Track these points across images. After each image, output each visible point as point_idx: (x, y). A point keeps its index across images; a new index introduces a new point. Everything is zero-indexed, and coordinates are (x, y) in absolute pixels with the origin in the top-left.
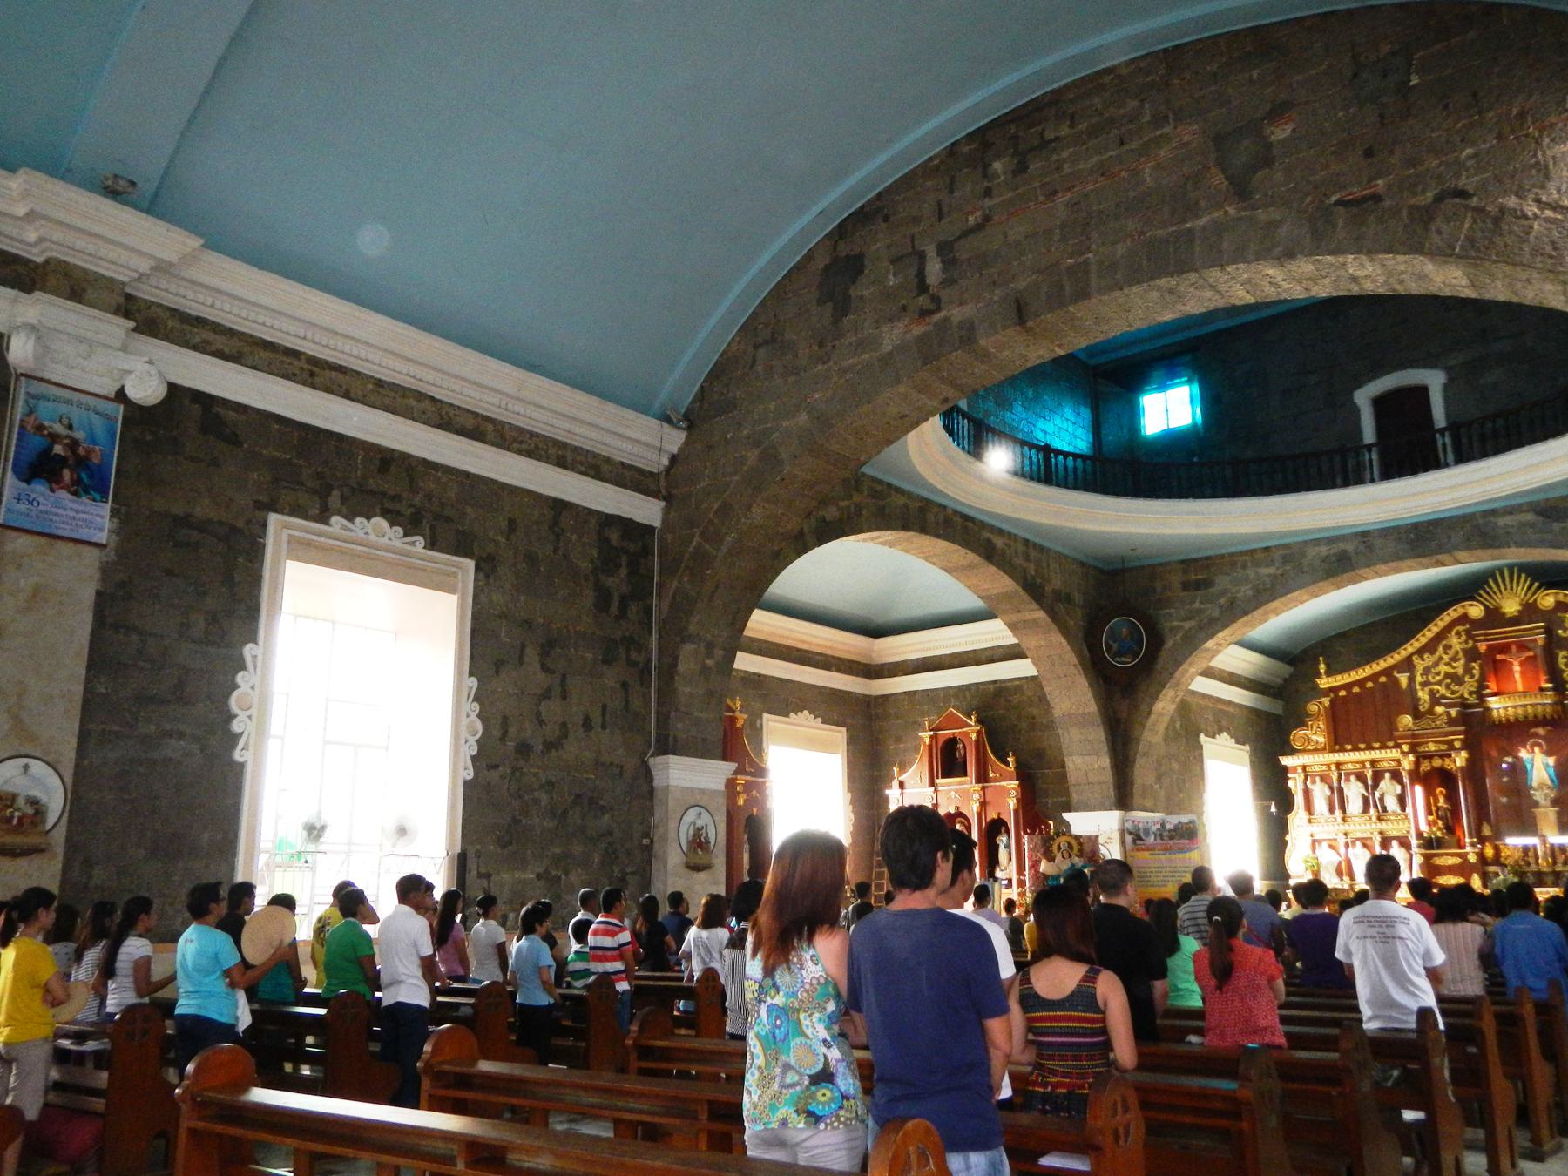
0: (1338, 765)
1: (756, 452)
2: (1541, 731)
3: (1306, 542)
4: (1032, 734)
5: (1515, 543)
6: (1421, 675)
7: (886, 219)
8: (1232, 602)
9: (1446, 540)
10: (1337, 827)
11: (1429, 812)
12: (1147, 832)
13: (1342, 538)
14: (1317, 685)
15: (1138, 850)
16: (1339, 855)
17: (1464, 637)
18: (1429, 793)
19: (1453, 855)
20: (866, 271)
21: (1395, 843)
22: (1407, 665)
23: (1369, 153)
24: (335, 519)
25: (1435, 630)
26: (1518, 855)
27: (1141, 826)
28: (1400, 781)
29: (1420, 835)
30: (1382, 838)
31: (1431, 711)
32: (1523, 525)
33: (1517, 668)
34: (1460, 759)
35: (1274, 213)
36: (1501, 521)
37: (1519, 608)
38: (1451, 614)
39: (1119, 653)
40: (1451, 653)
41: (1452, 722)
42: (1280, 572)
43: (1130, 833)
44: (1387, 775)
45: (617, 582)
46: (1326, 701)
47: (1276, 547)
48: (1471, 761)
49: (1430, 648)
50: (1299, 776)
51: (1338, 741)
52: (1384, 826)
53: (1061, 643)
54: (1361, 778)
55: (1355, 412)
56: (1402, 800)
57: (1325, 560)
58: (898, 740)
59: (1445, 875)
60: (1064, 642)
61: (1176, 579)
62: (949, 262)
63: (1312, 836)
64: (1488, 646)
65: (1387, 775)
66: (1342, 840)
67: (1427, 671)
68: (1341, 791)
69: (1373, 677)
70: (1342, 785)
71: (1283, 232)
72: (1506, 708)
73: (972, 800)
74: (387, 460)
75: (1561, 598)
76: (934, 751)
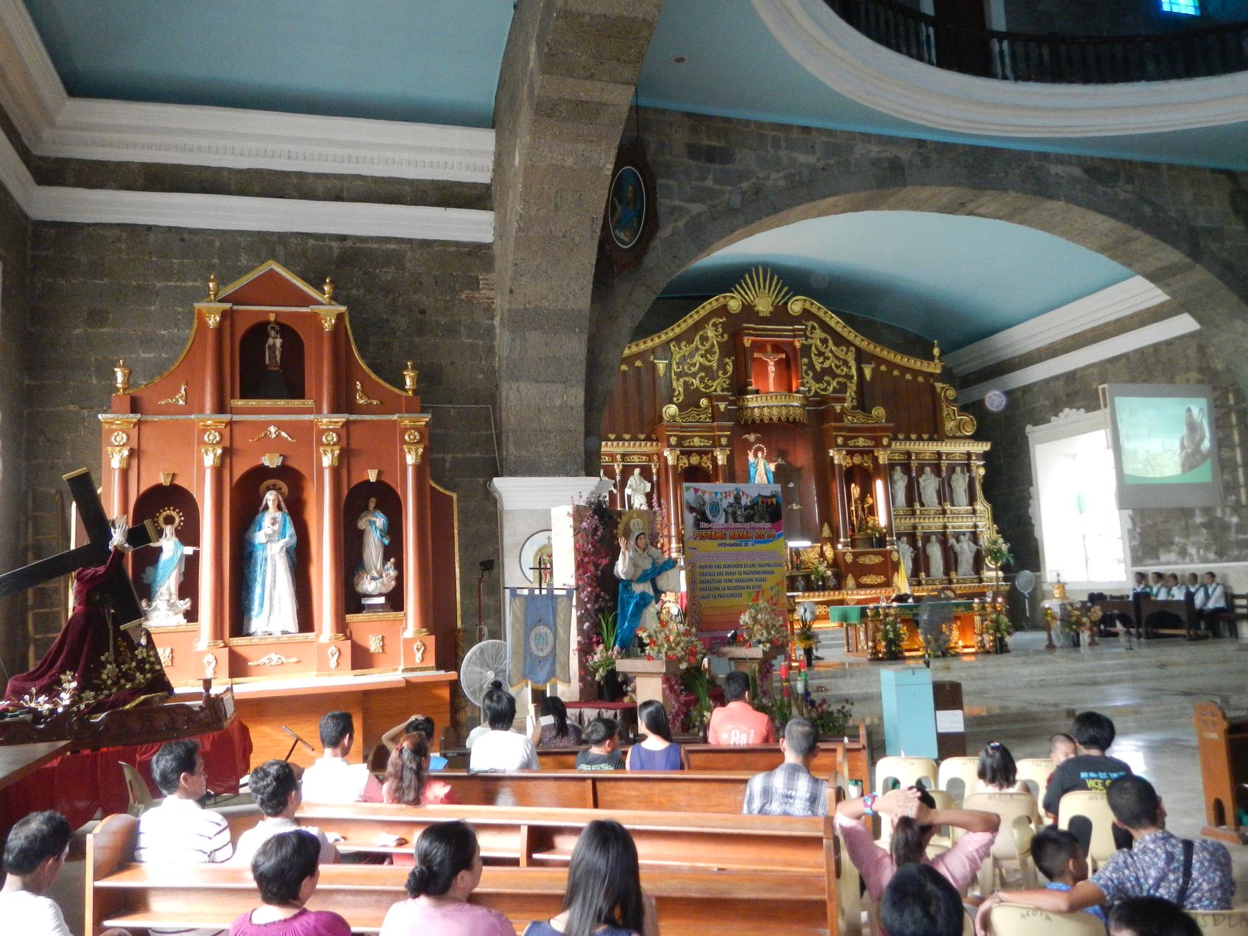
3: (852, 135)
4: (417, 340)
5: (1066, 197)
6: (678, 364)
9: (1003, 174)
12: (715, 507)
15: (702, 538)
17: (720, 330)
25: (696, 317)
27: (707, 497)
28: (650, 481)
33: (772, 368)
34: (721, 459)
37: (771, 309)
40: (708, 345)
42: (821, 164)
43: (692, 509)
44: (637, 471)
47: (818, 129)
49: (687, 336)
53: (600, 169)
57: (875, 163)
58: (96, 317)
61: (680, 138)
64: (753, 342)
65: (637, 471)
73: (322, 444)
75: (808, 306)
76: (227, 341)
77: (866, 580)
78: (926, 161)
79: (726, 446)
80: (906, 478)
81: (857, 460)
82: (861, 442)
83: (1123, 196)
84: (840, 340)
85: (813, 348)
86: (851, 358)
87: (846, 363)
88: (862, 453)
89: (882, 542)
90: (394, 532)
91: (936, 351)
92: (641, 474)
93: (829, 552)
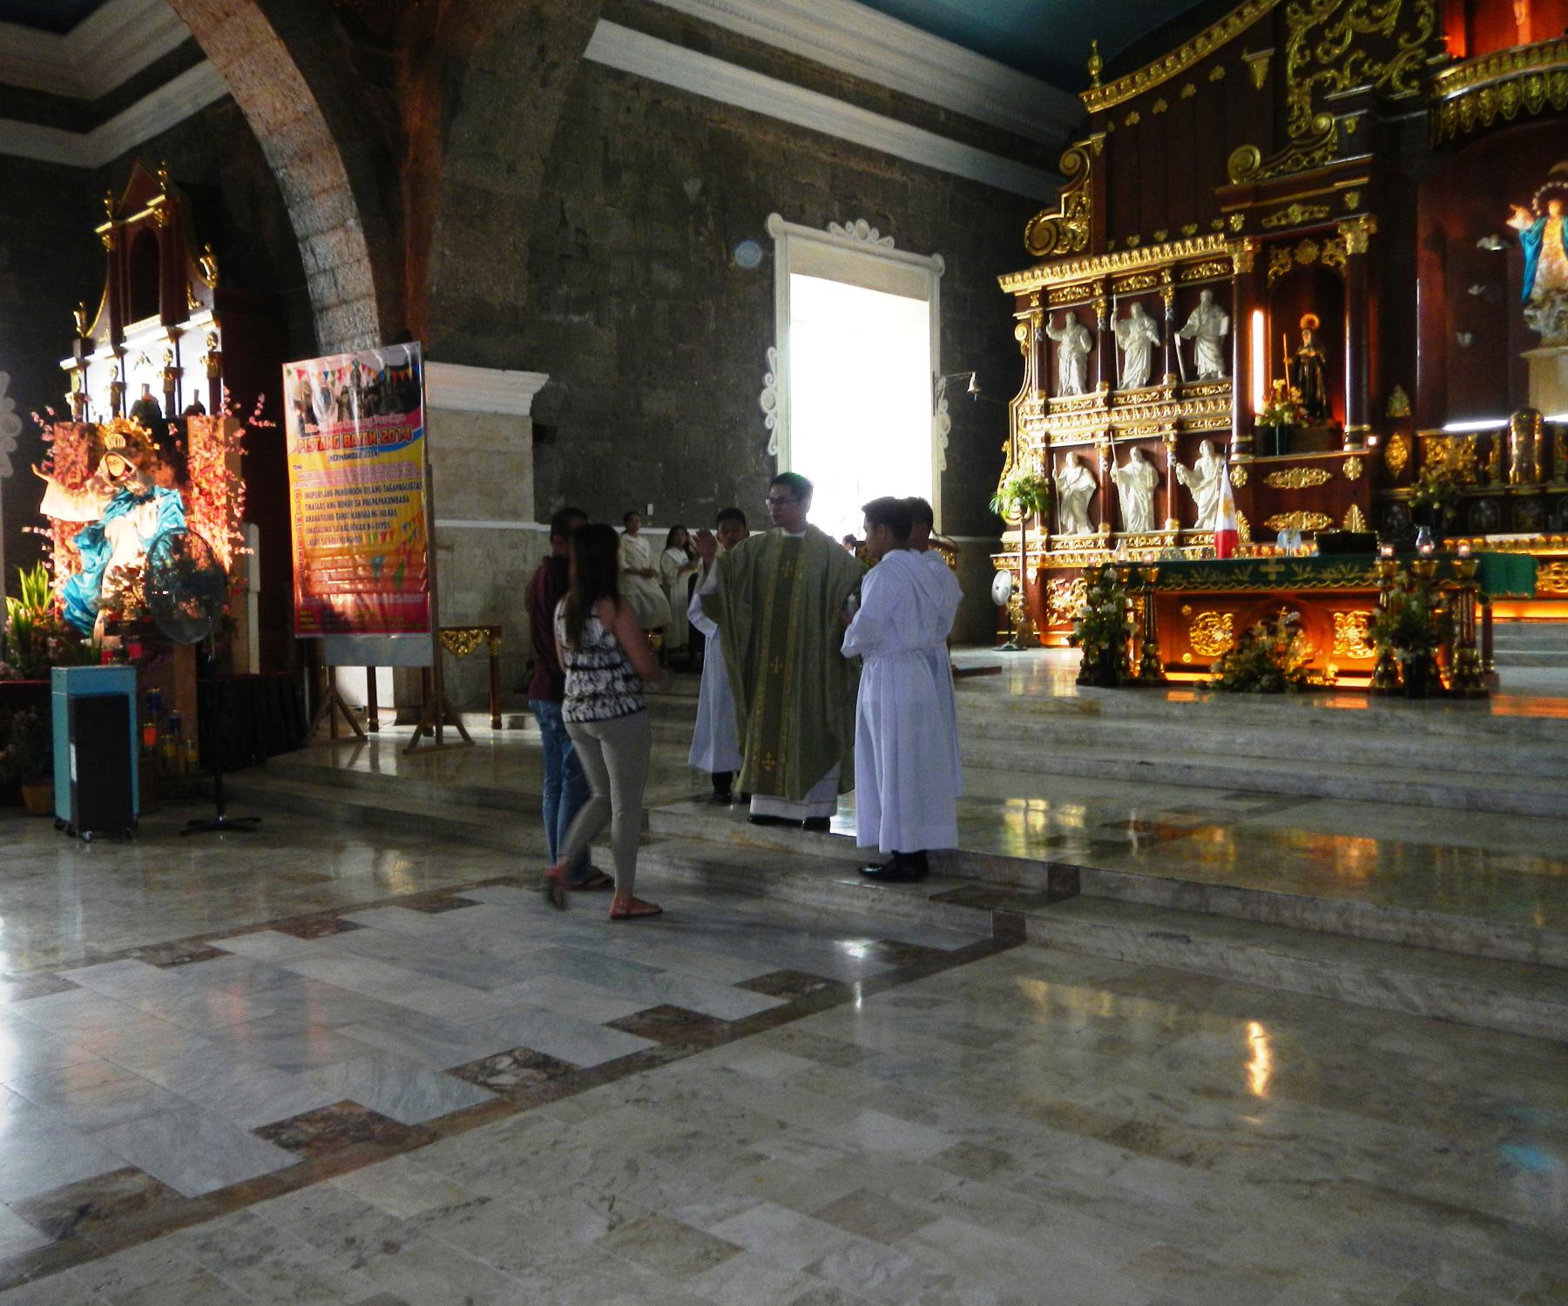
0: (1109, 282)
10: (1095, 419)
11: (1275, 369)
14: (1083, 106)
16: (1095, 477)
18: (1281, 329)
19: (1311, 464)
21: (1204, 448)
30: (1177, 436)
34: (1353, 241)
44: (1204, 295)
52: (1188, 410)
54: (1151, 306)
56: (1224, 349)
59: (1292, 512)
63: (1047, 438)
68: (1109, 337)
70: (1113, 327)
72: (1474, 94)
79: (1358, 210)
92: (1214, 301)
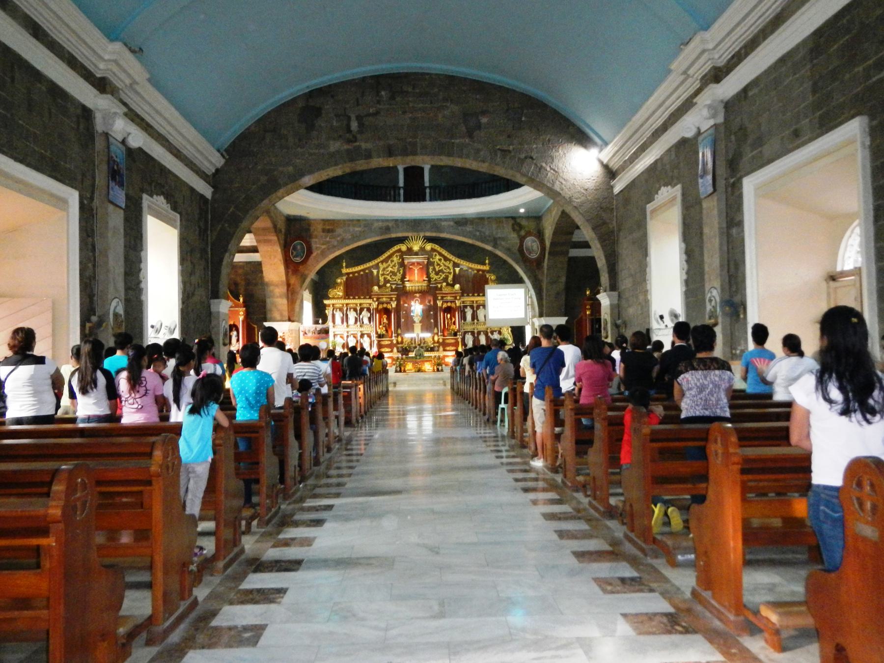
0: (347, 304)
1: (266, 178)
2: (418, 295)
7: (332, 96)
8: (342, 240)
11: (380, 324)
12: (309, 331)
13: (387, 220)
18: (380, 318)
20: (323, 115)
21: (366, 336)
22: (377, 266)
23: (509, 137)
24: (155, 196)
26: (409, 341)
28: (370, 312)
29: (377, 333)
31: (385, 285)
32: (449, 226)
33: (416, 272)
34: (394, 304)
35: (480, 146)
36: (443, 223)
38: (396, 248)
39: (296, 256)
40: (393, 263)
41: (392, 290)
45: (202, 224)
46: (344, 278)
48: (397, 305)
49: (386, 260)
50: (331, 308)
51: (348, 294)
54: (355, 310)
55: (397, 171)
56: (370, 319)
57: (381, 228)
60: (280, 250)
61: (320, 227)
62: (361, 125)
66: (345, 335)
67: (384, 269)
68: (347, 315)
69: (363, 270)
71: (482, 153)
74: (164, 171)
77: (448, 348)
78: (397, 226)
80: (471, 311)
81: (449, 304)
82: (449, 298)
83: (468, 229)
84: (446, 259)
85: (436, 263)
86: (451, 266)
87: (448, 268)
88: (451, 302)
89: (455, 334)
90: (238, 335)
91: (487, 261)
93: (436, 338)
